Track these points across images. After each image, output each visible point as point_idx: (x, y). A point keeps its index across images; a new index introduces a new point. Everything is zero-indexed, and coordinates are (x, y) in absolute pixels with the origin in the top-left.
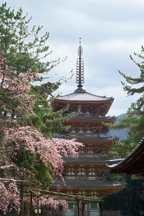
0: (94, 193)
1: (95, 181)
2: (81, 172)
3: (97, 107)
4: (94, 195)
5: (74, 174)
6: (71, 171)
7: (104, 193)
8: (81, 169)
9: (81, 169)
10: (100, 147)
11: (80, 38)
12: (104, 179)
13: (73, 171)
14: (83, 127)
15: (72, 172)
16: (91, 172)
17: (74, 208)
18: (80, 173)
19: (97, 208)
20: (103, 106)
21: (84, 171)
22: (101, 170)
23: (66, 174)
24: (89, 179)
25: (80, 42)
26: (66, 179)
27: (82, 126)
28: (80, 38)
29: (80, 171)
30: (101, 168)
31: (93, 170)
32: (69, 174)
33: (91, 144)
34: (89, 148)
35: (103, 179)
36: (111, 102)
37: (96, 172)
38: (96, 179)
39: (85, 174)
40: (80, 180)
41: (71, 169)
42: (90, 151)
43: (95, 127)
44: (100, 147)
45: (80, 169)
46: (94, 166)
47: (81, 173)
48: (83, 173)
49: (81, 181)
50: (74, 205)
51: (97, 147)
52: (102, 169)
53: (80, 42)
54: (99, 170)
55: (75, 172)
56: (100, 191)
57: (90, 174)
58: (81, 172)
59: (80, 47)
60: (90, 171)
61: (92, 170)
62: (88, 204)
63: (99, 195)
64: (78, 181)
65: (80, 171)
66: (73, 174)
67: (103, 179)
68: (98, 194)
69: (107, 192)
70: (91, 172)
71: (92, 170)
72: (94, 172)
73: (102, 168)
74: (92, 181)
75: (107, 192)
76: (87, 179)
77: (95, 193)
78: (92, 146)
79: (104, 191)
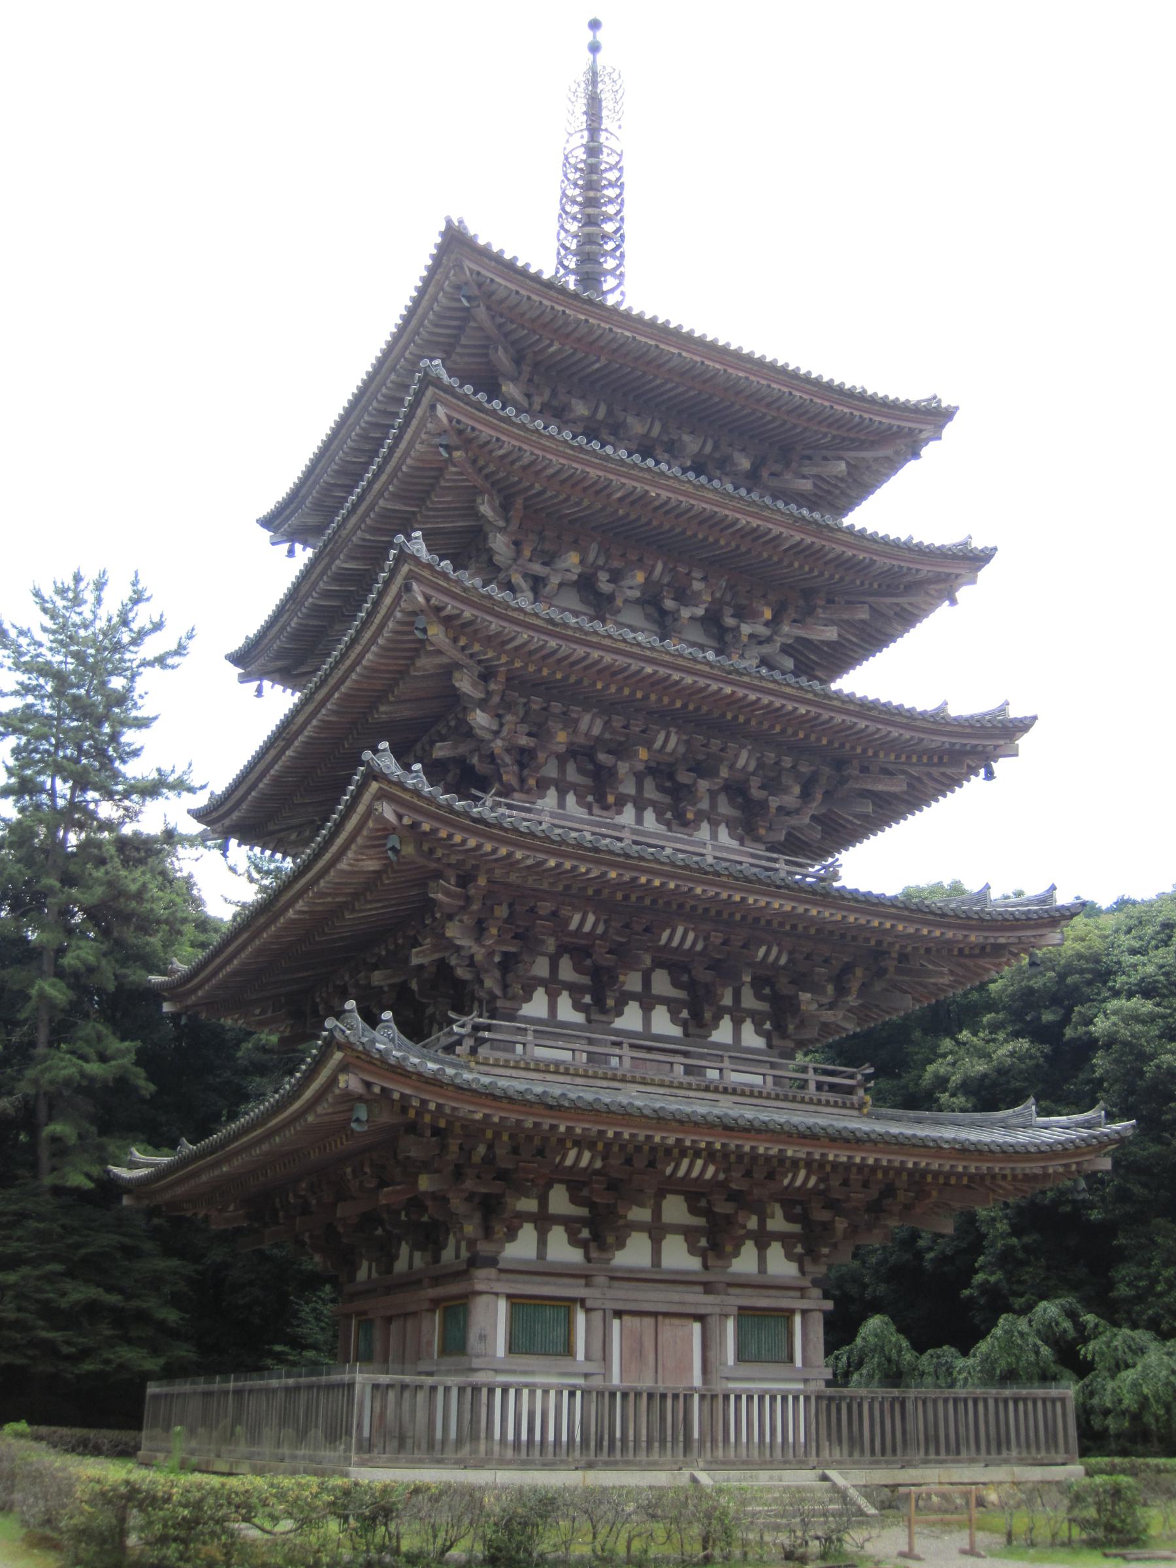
2: (647, 1009)
3: (777, 468)
11: (595, 25)
13: (575, 990)
15: (565, 994)
16: (727, 1018)
17: (580, 1354)
18: (630, 1019)
19: (791, 1359)
23: (508, 1004)
25: (594, 48)
28: (595, 25)
29: (633, 996)
32: (536, 1007)
35: (850, 1090)
40: (667, 1079)
47: (647, 1021)
48: (663, 1024)
50: (580, 1318)
53: (594, 48)
58: (647, 1009)
59: (595, 74)
66: (567, 1011)
67: (850, 1090)
70: (727, 1018)
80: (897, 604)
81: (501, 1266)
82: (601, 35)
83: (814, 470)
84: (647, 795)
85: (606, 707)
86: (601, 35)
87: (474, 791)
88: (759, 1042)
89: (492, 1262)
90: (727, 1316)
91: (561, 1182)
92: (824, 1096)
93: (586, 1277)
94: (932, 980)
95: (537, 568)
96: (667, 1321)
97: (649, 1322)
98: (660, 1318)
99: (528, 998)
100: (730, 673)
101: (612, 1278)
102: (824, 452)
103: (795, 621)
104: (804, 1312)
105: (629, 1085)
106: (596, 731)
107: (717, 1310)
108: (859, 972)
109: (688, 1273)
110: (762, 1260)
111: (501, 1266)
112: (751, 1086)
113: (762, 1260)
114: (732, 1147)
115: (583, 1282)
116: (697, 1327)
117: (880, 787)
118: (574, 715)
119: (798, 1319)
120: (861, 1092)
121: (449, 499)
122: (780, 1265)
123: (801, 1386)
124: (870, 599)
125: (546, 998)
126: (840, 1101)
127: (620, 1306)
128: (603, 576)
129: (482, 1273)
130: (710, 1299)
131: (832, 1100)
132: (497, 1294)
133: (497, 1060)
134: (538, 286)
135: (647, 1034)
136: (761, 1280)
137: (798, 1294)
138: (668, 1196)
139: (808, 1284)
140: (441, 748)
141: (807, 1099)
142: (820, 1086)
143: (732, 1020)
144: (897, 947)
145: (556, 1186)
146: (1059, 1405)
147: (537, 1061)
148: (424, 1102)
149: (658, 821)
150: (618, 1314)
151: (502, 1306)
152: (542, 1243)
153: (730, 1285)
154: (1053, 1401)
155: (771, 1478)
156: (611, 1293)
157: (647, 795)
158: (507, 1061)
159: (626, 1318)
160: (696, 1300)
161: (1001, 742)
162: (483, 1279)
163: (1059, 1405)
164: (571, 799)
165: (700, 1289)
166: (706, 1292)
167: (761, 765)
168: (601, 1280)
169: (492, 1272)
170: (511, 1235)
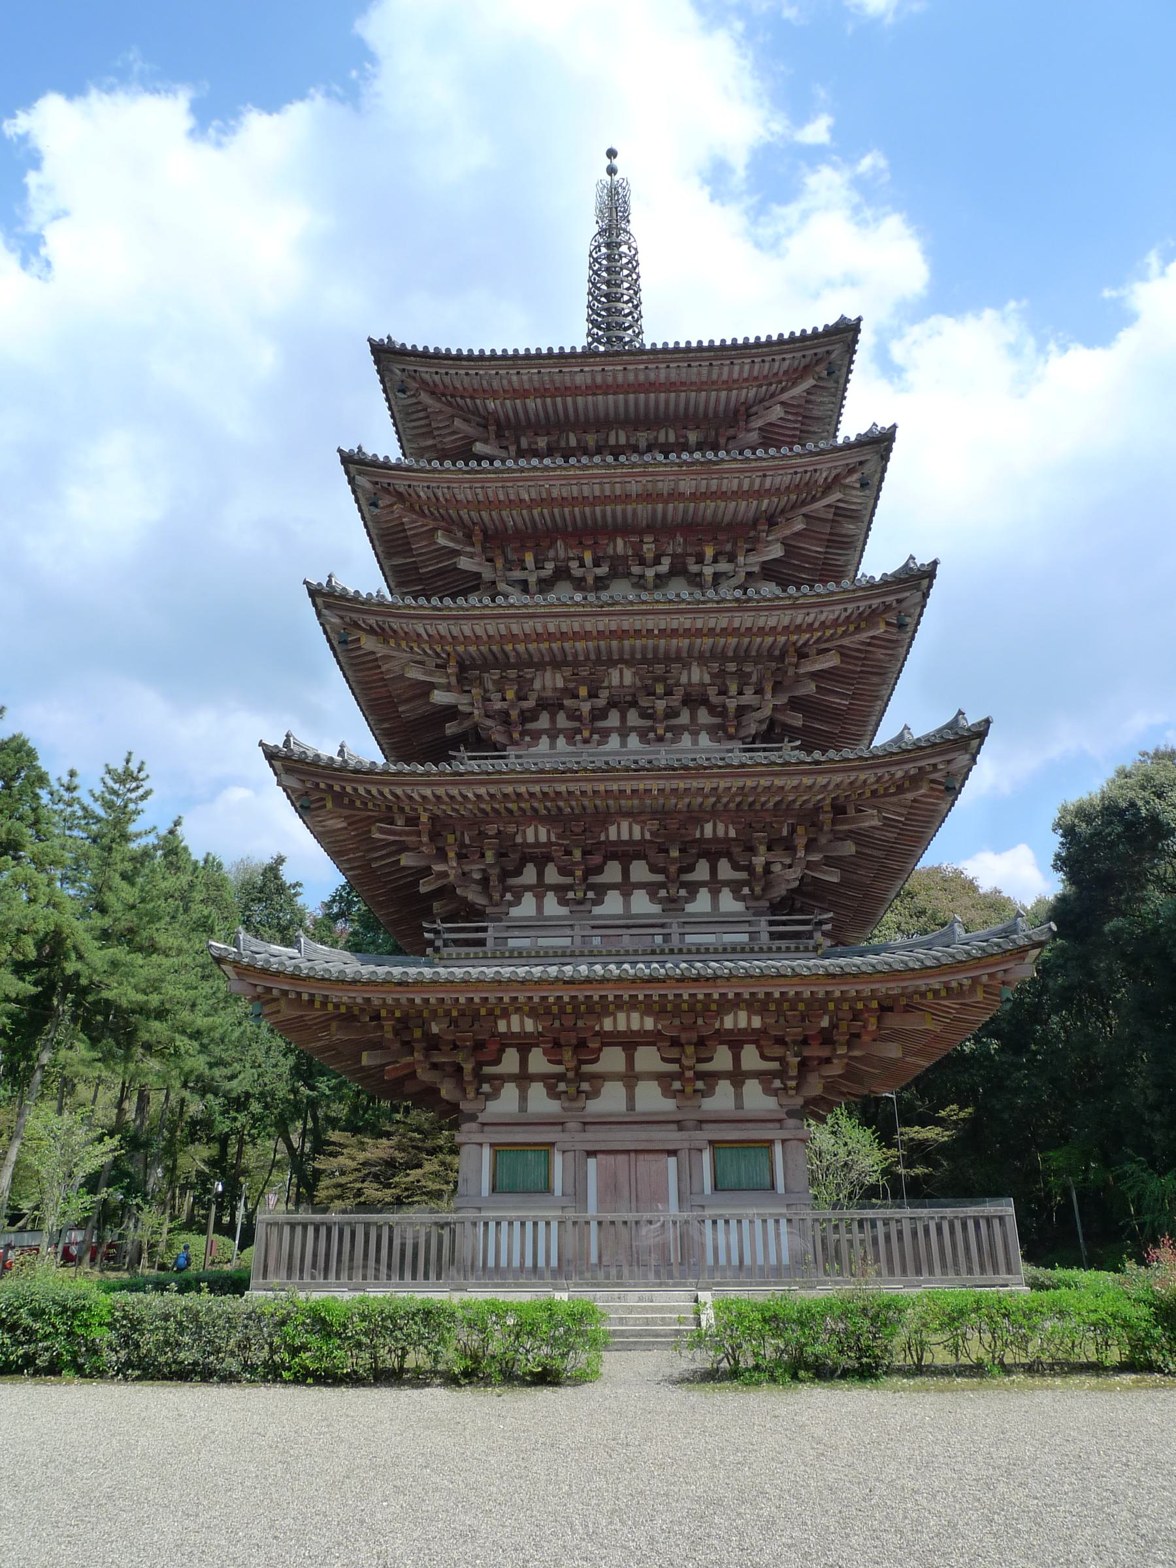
0: (737, 1059)
1: (743, 951)
3: (731, 432)
4: (737, 1077)
5: (564, 911)
6: (540, 889)
7: (825, 1052)
8: (626, 873)
9: (626, 873)
10: (768, 688)
11: (611, 154)
12: (818, 936)
14: (636, 570)
17: (558, 1191)
18: (613, 904)
19: (773, 1187)
20: (777, 413)
21: (652, 889)
22: (790, 866)
23: (496, 910)
24: (689, 939)
25: (611, 171)
26: (490, 943)
27: (629, 575)
28: (611, 154)
29: (613, 886)
30: (789, 847)
31: (725, 870)
32: (527, 907)
33: (697, 675)
34: (684, 718)
36: (833, 356)
37: (746, 890)
38: (753, 935)
39: (656, 909)
41: (541, 875)
42: (695, 734)
43: (723, 566)
44: (768, 688)
45: (612, 872)
46: (732, 834)
47: (627, 904)
48: (642, 903)
49: (618, 954)
50: (558, 1159)
51: (749, 698)
52: (801, 853)
53: (611, 171)
54: (777, 868)
55: (571, 895)
56: (794, 1032)
57: (702, 903)
60: (702, 884)
61: (714, 871)
62: (684, 1155)
63: (781, 1074)
64: (591, 954)
65: (613, 886)
68: (774, 1065)
69: (858, 1036)
71: (714, 871)
72: (736, 887)
73: (801, 842)
74: (716, 951)
75: (858, 1036)
76: (675, 939)
77: (751, 1058)
78: (705, 702)
79: (826, 1038)
80: (829, 506)
81: (482, 1118)
82: (616, 162)
83: (759, 423)
84: (629, 724)
85: (557, 663)
86: (616, 162)
87: (451, 753)
88: (739, 906)
89: (472, 1118)
90: (701, 1151)
91: (510, 1045)
92: (777, 943)
93: (562, 1124)
94: (867, 824)
95: (517, 574)
96: (641, 1157)
97: (622, 1158)
98: (633, 1155)
99: (517, 901)
100: (602, 607)
101: (585, 1124)
102: (766, 404)
103: (749, 551)
104: (784, 1141)
105: (579, 958)
106: (560, 684)
107: (686, 1145)
108: (800, 830)
109: (664, 1113)
110: (739, 1097)
111: (482, 1118)
112: (700, 944)
113: (739, 1097)
114: (581, 998)
115: (560, 1128)
116: (672, 1161)
117: (818, 667)
118: (529, 676)
119: (778, 1149)
120: (818, 936)
121: (424, 543)
122: (756, 1098)
123: (784, 1211)
124: (804, 510)
125: (534, 899)
126: (792, 946)
127: (590, 1147)
128: (574, 565)
129: (465, 1127)
130: (684, 1135)
131: (783, 947)
132: (481, 1145)
133: (476, 953)
134: (450, 362)
135: (627, 915)
136: (740, 1114)
137: (778, 1125)
138: (640, 1048)
139: (785, 1116)
140: (450, 727)
141: (756, 949)
142: (773, 936)
143: (710, 892)
144: (828, 801)
145: (507, 1050)
146: (996, 1223)
147: (512, 951)
148: (299, 994)
149: (640, 742)
150: (591, 1153)
151: (487, 1152)
152: (523, 1098)
153: (701, 1122)
154: (988, 1220)
155: (640, 1300)
156: (588, 1136)
157: (629, 724)
158: (468, 954)
159: (600, 1156)
160: (670, 1137)
161: (907, 594)
162: (466, 1134)
163: (996, 1223)
164: (561, 742)
165: (674, 1127)
166: (680, 1129)
167: (713, 676)
168: (571, 1125)
169: (473, 1126)
170: (494, 1095)
